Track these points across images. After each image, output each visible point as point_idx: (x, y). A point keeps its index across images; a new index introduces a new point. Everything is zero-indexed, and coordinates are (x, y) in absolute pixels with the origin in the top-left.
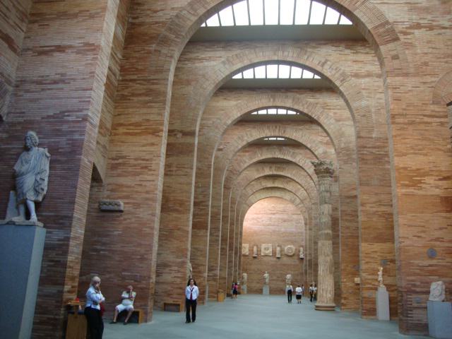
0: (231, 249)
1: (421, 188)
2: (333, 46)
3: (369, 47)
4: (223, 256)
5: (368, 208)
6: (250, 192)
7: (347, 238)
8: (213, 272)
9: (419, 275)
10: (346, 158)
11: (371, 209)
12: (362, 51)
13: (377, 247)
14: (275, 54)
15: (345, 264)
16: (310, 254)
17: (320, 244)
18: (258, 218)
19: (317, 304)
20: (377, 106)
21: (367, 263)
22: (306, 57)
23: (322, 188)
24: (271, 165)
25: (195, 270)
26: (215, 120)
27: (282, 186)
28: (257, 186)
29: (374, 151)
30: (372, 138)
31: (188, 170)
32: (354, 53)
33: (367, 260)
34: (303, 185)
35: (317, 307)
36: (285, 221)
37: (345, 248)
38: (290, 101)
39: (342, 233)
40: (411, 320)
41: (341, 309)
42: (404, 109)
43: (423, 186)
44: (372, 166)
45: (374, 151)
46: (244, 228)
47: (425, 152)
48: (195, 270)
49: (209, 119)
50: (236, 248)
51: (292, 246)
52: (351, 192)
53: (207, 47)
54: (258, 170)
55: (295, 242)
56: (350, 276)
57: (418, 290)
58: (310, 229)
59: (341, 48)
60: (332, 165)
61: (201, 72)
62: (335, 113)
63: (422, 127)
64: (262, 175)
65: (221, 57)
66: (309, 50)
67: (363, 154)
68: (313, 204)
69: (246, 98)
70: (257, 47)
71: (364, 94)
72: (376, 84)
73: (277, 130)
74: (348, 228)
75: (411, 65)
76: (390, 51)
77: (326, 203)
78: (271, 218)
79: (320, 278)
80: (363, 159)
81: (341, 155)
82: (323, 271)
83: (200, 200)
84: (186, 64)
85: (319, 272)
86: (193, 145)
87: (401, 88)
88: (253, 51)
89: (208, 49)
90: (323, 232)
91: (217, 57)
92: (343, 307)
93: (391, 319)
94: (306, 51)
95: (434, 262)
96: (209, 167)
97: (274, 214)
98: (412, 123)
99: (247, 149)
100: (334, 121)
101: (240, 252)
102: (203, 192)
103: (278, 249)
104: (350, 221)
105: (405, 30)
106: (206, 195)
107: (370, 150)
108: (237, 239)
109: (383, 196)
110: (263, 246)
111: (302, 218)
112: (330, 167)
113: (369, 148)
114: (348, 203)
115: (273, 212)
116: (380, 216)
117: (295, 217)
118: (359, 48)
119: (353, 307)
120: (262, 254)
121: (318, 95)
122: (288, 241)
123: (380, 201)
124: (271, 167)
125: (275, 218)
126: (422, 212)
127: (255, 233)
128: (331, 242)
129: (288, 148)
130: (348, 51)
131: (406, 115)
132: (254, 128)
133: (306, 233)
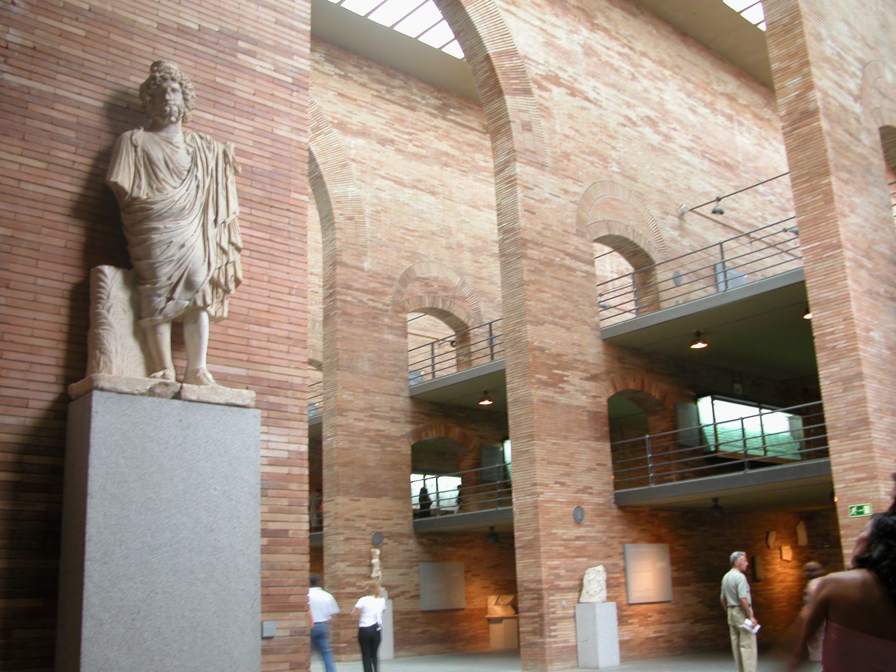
1: (563, 392)
5: (350, 420)
9: (563, 556)
11: (356, 423)
12: (355, 78)
13: (365, 505)
20: (374, 205)
21: (348, 539)
29: (365, 298)
30: (362, 270)
32: (340, 75)
33: (348, 533)
40: (555, 642)
42: (538, 233)
43: (567, 387)
44: (359, 331)
45: (365, 300)
47: (568, 322)
57: (563, 584)
63: (563, 274)
71: (354, 171)
72: (376, 156)
75: (549, 150)
76: (520, 111)
87: (536, 190)
93: (396, 657)
95: (580, 531)
98: (549, 263)
105: (538, 78)
107: (359, 294)
109: (377, 398)
113: (357, 290)
116: (372, 440)
123: (372, 408)
126: (566, 438)
130: (328, 68)
131: (542, 245)
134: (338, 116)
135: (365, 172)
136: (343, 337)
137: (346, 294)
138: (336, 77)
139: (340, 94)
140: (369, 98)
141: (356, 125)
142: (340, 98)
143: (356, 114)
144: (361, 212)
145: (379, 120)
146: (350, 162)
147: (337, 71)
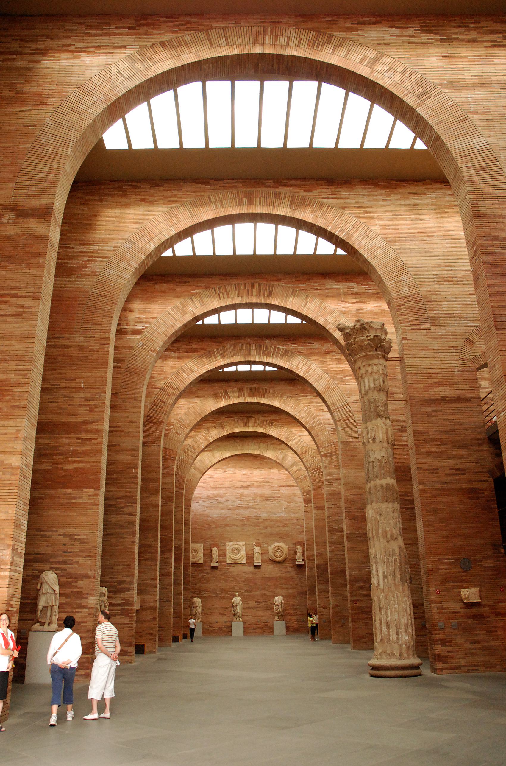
0: (165, 548)
2: (392, 27)
3: (475, 28)
4: (149, 562)
6: (204, 444)
7: (435, 496)
8: (123, 595)
10: (416, 317)
12: (461, 37)
14: (256, 42)
15: (435, 558)
16: (319, 555)
17: (370, 512)
18: (217, 495)
19: (374, 662)
22: (330, 49)
23: (368, 383)
24: (240, 385)
25: (68, 591)
26: (119, 243)
27: (261, 430)
28: (215, 434)
31: (28, 302)
32: (441, 40)
34: (303, 421)
35: (374, 668)
36: (267, 499)
37: (431, 518)
38: (287, 202)
39: (421, 483)
41: (434, 670)
46: (192, 513)
48: (68, 591)
49: (106, 242)
50: (178, 548)
51: (282, 544)
52: (431, 392)
53: (91, 27)
54: (216, 396)
55: (287, 535)
56: (449, 585)
58: (316, 507)
59: (411, 31)
60: (386, 333)
61: (74, 79)
62: (384, 227)
64: (223, 403)
65: (125, 47)
66: (336, 34)
67: (491, 253)
68: (325, 455)
69: (189, 199)
70: (211, 28)
71: (478, 123)
73: (255, 292)
74: (434, 471)
77: (379, 416)
78: (241, 495)
79: (378, 596)
80: (495, 266)
81: (404, 311)
82: (385, 577)
83: (80, 420)
84: (39, 61)
85: (374, 581)
86: (43, 239)
88: (202, 35)
89: (93, 32)
90: (378, 482)
91: (115, 48)
92: (439, 666)
94: (331, 36)
96: (104, 342)
97: (247, 487)
99: (194, 346)
100: (383, 243)
101: (187, 558)
102: (87, 400)
103: (257, 550)
104: (438, 455)
106: (96, 406)
108: (178, 532)
110: (230, 546)
111: (297, 491)
112: (383, 337)
114: (429, 415)
115: (245, 484)
117: (284, 491)
118: (454, 30)
119: (463, 662)
120: (228, 561)
121: (343, 192)
122: (272, 535)
124: (241, 389)
125: (248, 496)
127: (215, 513)
128: (397, 505)
129: (274, 342)
130: (426, 37)
132: (207, 288)
133: (308, 518)
134: (447, 76)
135: (492, 120)
136: (497, 292)
137: (492, 246)
138: (439, 43)
139: (445, 57)
140: (482, 51)
141: (471, 79)
142: (446, 60)
143: (469, 70)
144: (496, 160)
145: (498, 67)
146: (471, 115)
147: (438, 37)
